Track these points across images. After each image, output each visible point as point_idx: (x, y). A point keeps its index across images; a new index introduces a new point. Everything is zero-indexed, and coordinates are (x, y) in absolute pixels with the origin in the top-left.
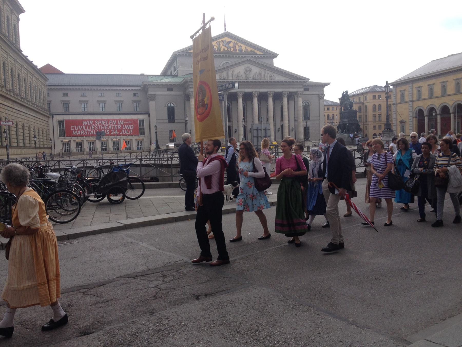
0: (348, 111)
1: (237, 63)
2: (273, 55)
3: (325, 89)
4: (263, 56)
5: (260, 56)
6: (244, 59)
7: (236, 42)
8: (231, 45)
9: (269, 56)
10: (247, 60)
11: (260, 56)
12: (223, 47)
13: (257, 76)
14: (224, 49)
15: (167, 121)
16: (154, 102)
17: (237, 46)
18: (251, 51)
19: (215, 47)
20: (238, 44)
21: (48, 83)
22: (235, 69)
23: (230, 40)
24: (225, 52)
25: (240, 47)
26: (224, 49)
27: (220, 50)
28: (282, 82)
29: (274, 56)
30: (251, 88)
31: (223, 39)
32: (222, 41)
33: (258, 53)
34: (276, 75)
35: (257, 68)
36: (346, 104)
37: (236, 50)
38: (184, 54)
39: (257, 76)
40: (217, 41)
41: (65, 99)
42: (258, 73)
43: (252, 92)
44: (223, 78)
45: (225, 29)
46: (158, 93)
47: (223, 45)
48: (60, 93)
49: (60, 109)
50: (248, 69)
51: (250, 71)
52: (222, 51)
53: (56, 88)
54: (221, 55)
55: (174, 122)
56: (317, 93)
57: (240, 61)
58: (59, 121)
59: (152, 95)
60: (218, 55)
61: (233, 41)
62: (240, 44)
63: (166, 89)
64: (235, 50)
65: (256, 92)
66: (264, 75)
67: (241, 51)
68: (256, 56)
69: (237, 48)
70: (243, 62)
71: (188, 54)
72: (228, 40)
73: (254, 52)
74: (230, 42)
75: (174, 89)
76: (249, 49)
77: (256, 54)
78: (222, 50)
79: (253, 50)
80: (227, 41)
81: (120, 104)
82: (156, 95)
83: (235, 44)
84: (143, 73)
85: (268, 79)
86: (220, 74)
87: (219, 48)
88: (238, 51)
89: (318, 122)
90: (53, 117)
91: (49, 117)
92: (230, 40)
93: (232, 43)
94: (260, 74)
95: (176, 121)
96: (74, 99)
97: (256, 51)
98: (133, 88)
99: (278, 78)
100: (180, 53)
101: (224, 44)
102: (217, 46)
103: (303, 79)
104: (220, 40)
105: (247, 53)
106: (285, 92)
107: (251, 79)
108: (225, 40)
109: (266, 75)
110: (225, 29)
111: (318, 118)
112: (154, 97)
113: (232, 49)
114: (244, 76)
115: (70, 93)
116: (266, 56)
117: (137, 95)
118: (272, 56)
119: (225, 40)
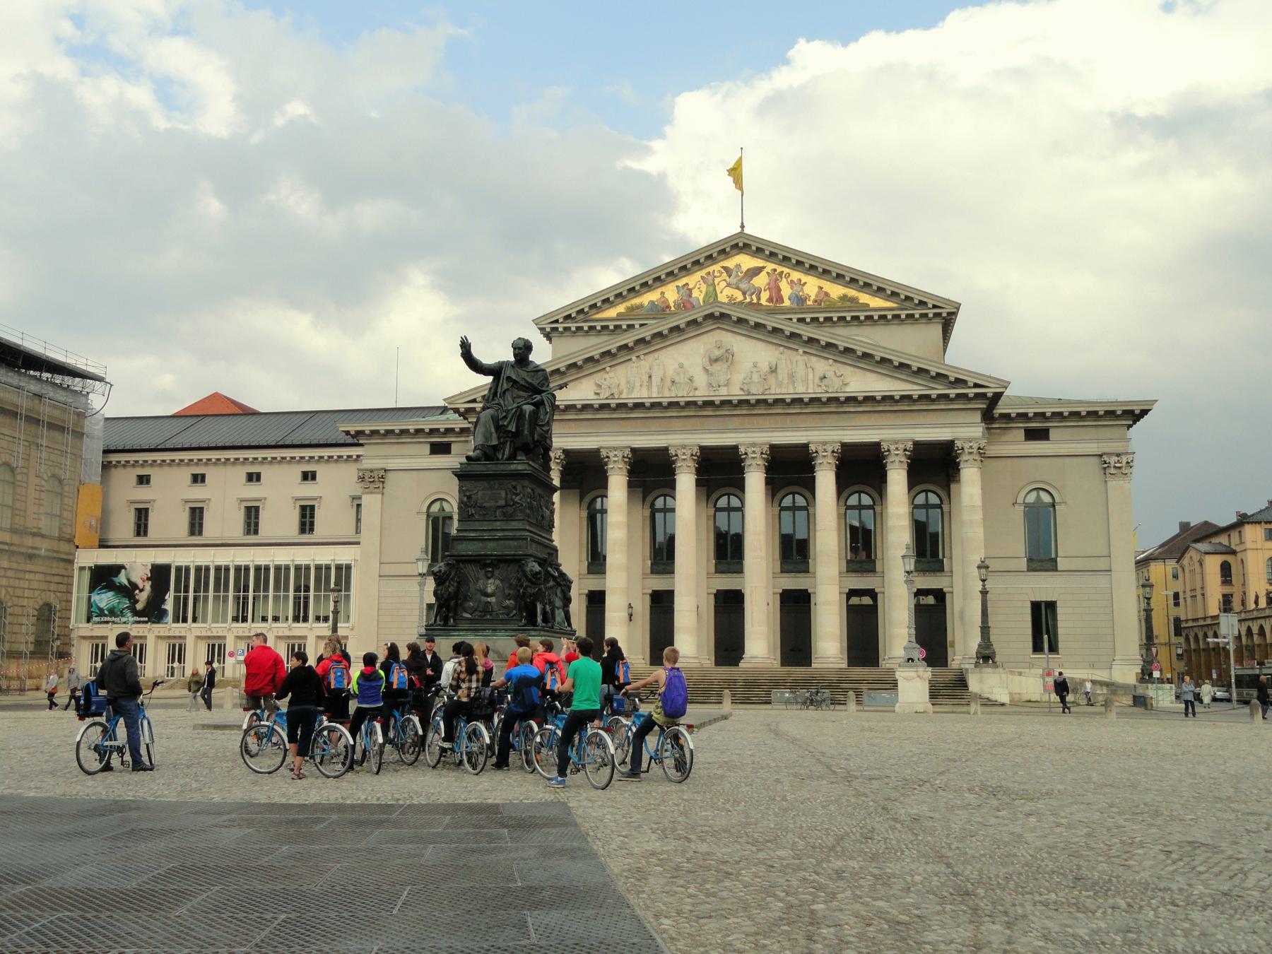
2: (935, 307)
7: (779, 269)
8: (761, 281)
9: (917, 313)
19: (695, 294)
25: (797, 288)
26: (731, 298)
31: (731, 263)
34: (847, 371)
37: (781, 299)
38: (573, 326)
39: (756, 377)
40: (703, 273)
42: (764, 367)
44: (605, 394)
45: (742, 227)
46: (392, 464)
47: (729, 285)
50: (717, 353)
56: (1093, 448)
59: (372, 471)
61: (770, 266)
62: (796, 275)
63: (427, 448)
64: (777, 297)
65: (754, 445)
66: (792, 376)
67: (800, 300)
68: (862, 316)
69: (786, 291)
72: (746, 261)
73: (854, 300)
74: (756, 271)
77: (865, 307)
80: (744, 269)
86: (598, 378)
87: (712, 295)
88: (787, 303)
89: (1101, 582)
92: (758, 263)
93: (763, 274)
100: (557, 321)
101: (733, 280)
103: (976, 386)
104: (716, 267)
107: (735, 393)
108: (738, 266)
109: (801, 371)
110: (742, 227)
111: (1102, 564)
113: (765, 296)
114: (701, 380)
118: (931, 313)
119: (738, 266)
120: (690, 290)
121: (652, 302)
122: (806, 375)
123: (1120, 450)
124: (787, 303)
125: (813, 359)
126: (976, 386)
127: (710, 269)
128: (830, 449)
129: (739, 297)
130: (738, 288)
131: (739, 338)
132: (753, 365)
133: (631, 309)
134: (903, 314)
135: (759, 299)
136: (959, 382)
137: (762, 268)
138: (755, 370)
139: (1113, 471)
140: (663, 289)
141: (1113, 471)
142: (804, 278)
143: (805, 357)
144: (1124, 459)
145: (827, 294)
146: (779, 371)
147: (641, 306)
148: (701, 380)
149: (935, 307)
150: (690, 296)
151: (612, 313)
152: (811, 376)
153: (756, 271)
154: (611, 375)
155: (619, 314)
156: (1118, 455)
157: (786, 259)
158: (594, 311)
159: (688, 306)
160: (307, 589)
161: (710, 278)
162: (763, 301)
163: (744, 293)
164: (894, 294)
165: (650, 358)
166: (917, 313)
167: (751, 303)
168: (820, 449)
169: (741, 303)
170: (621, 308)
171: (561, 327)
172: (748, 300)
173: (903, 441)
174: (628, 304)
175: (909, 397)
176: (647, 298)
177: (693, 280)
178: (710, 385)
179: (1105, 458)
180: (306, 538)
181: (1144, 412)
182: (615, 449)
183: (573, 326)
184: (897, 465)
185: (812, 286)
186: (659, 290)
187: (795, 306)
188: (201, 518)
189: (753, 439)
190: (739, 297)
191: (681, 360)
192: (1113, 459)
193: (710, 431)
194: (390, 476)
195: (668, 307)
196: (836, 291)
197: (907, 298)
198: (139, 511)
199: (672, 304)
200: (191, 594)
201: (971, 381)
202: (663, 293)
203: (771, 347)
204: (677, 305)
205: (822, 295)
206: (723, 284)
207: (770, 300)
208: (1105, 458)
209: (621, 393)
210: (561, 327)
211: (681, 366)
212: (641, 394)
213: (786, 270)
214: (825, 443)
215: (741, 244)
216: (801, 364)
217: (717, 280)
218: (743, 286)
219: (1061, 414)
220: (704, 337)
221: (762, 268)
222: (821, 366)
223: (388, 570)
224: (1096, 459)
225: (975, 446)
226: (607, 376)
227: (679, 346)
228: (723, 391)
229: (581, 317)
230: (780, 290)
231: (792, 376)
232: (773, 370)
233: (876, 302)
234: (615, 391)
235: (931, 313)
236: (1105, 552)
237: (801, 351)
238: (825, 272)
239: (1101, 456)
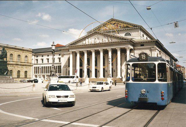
4: (132, 28)
23: (115, 22)
33: (130, 26)
62: (120, 24)
72: (114, 22)
74: (115, 23)
77: (129, 27)
79: (128, 25)
97: (129, 26)
99: (114, 40)
103: (127, 40)
126: (127, 40)
136: (125, 39)
153: (115, 23)
212: (87, 43)
233: (130, 26)
234: (85, 43)
235: (138, 27)
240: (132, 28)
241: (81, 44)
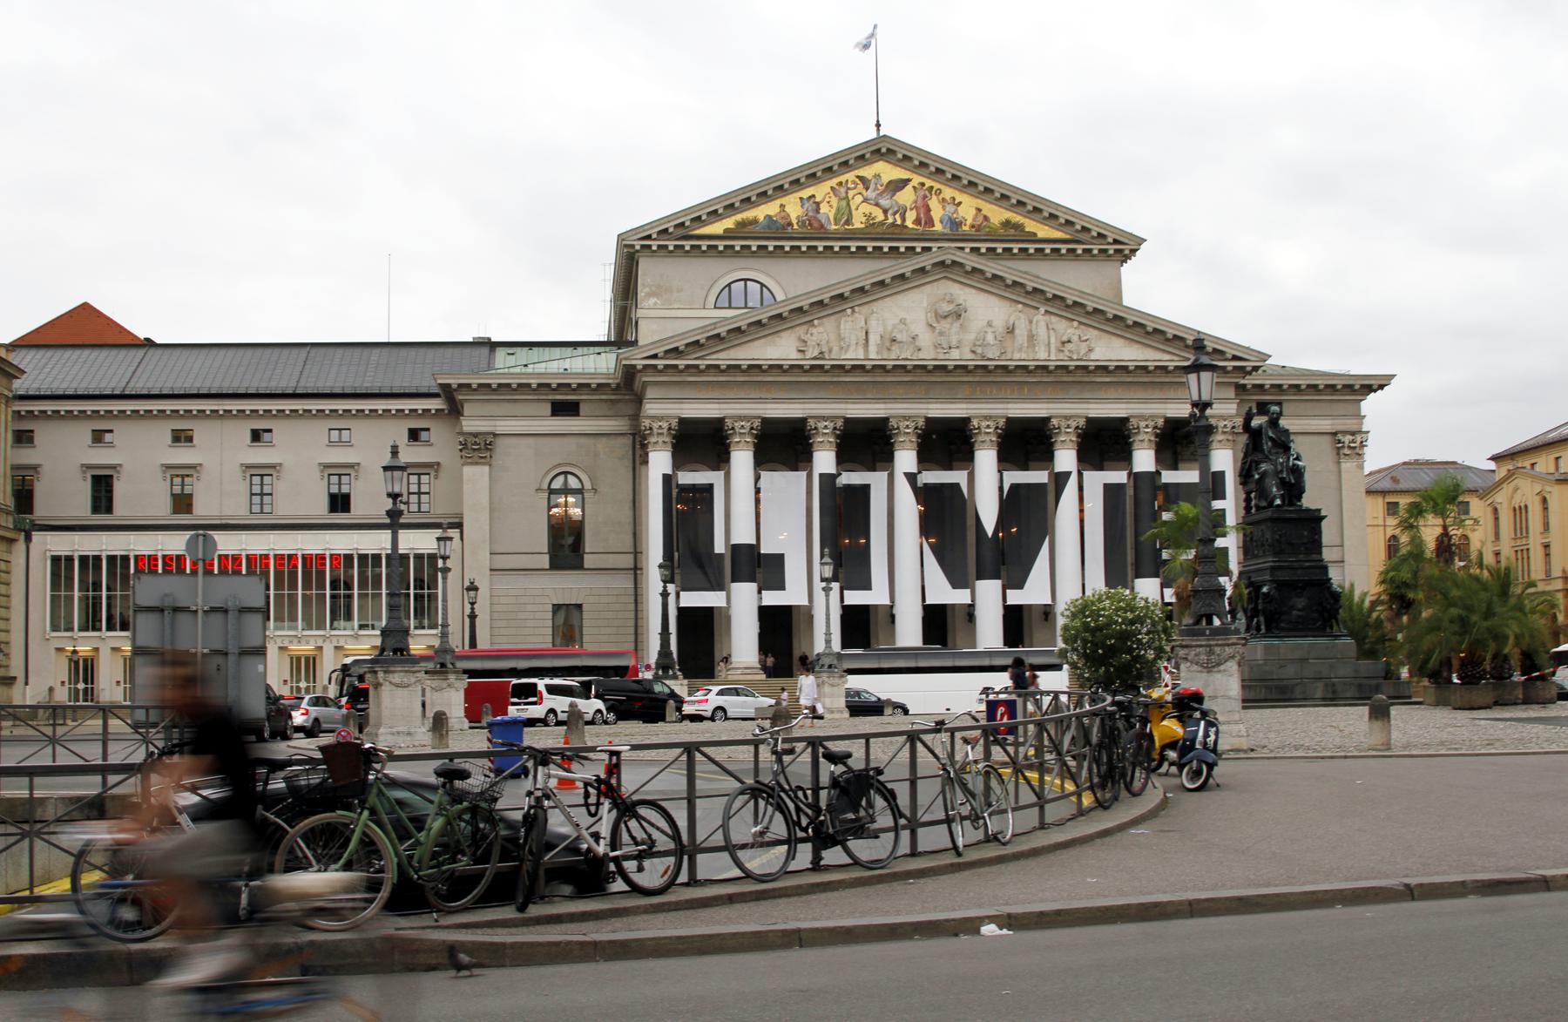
0: (1268, 514)
1: (887, 277)
2: (1116, 242)
3: (1371, 405)
4: (1064, 248)
5: (1048, 248)
6: (926, 261)
7: (929, 183)
8: (906, 197)
9: (1095, 249)
10: (942, 263)
11: (1048, 248)
12: (866, 208)
13: (990, 338)
14: (869, 216)
15: (545, 561)
16: (486, 468)
17: (934, 203)
18: (1007, 224)
19: (824, 208)
20: (939, 192)
21: (20, 386)
22: (876, 306)
23: (898, 173)
24: (872, 231)
25: (951, 208)
26: (869, 216)
27: (848, 222)
28: (1125, 368)
29: (1121, 248)
30: (968, 399)
31: (867, 172)
32: (861, 178)
33: (1044, 232)
35: (993, 300)
36: (1263, 475)
37: (930, 222)
39: (990, 338)
41: (101, 457)
43: (967, 420)
45: (878, 125)
46: (503, 426)
47: (866, 200)
48: (84, 431)
49: (79, 504)
51: (958, 314)
52: (857, 225)
53: (63, 406)
54: (853, 245)
55: (578, 565)
56: (1326, 425)
57: (906, 266)
58: (56, 560)
59: (476, 435)
60: (837, 245)
61: (917, 179)
62: (948, 193)
63: (547, 409)
65: (987, 418)
66: (1031, 337)
67: (955, 224)
68: (1032, 248)
69: (937, 213)
70: (922, 270)
71: (687, 245)
72: (887, 171)
73: (1018, 227)
74: (900, 185)
75: (583, 408)
76: (998, 215)
77: (1032, 238)
78: (858, 223)
79: (1017, 218)
80: (885, 179)
81: (345, 479)
82: (495, 435)
83: (925, 193)
84: (483, 334)
85: (1044, 354)
86: (801, 331)
87: (846, 215)
88: (938, 227)
90: (28, 539)
91: (12, 541)
92: (898, 173)
93: (909, 188)
94: (1011, 331)
95: (588, 561)
96: (141, 457)
97: (1031, 226)
98: (407, 405)
100: (649, 237)
102: (834, 201)
103: (1235, 358)
104: (850, 176)
105: (981, 231)
106: (1143, 417)
108: (877, 176)
109: (1042, 332)
110: (878, 125)
112: (488, 447)
114: (926, 339)
115: (200, 430)
116: (1080, 249)
117: (424, 435)
118: (1111, 249)
119: (877, 176)
120: (818, 204)
121: (769, 217)
122: (1045, 339)
123: (1355, 428)
124: (938, 227)
125: (1054, 319)
126: (1235, 358)
127: (843, 178)
128: (1074, 424)
129: (881, 217)
130: (877, 205)
131: (968, 290)
132: (986, 322)
133: (742, 224)
134: (1080, 249)
135: (904, 220)
137: (909, 180)
138: (990, 330)
139: (1346, 451)
140: (783, 201)
141: (1346, 451)
142: (959, 197)
143: (1047, 317)
144: (1359, 439)
145: (986, 218)
146: (1017, 332)
147: (755, 221)
148: (926, 339)
149: (1116, 242)
150: (817, 210)
151: (717, 228)
152: (1053, 340)
153: (900, 185)
154: (821, 329)
155: (726, 230)
156: (1353, 434)
157: (939, 171)
158: (696, 224)
159: (816, 225)
160: (349, 586)
161: (843, 190)
162: (909, 223)
163: (885, 212)
164: (1069, 223)
165: (865, 309)
166: (1095, 249)
167: (893, 225)
168: (1063, 424)
169: (882, 223)
170: (729, 223)
171: (654, 245)
172: (890, 220)
173: (1152, 417)
174: (739, 217)
175: (1164, 368)
176: (761, 212)
177: (821, 191)
178: (937, 346)
179: (1340, 437)
180: (340, 518)
181: (1381, 387)
182: (824, 418)
183: (671, 245)
184: (1146, 444)
185: (968, 208)
186: (778, 202)
187: (947, 231)
188: (110, 491)
189: (987, 412)
190: (881, 217)
191: (902, 315)
192: (1348, 438)
193: (937, 399)
194: (500, 442)
195: (790, 224)
196: (998, 215)
197: (1084, 229)
198: (97, 480)
199: (795, 222)
200: (104, 593)
201: (1230, 352)
202: (782, 206)
203: (1006, 304)
204: (802, 223)
205: (980, 219)
206: (859, 199)
207: (917, 221)
208: (1340, 437)
209: (830, 351)
210: (654, 245)
211: (903, 321)
212: (854, 355)
213: (937, 186)
214: (1067, 418)
215: (883, 149)
216: (1042, 325)
217: (851, 193)
218: (884, 202)
219: (1297, 386)
220: (928, 288)
221: (909, 180)
222: (1066, 329)
223: (501, 562)
224: (1328, 439)
225: (1230, 425)
226: (814, 331)
227: (899, 297)
228: (955, 354)
229: (681, 232)
230: (928, 210)
231: (1031, 337)
232: (1011, 331)
233: (1044, 232)
235: (1111, 249)
236: (1337, 542)
237: (1042, 310)
238: (988, 190)
239: (1335, 434)
240: (1064, 248)
241: (781, 349)
